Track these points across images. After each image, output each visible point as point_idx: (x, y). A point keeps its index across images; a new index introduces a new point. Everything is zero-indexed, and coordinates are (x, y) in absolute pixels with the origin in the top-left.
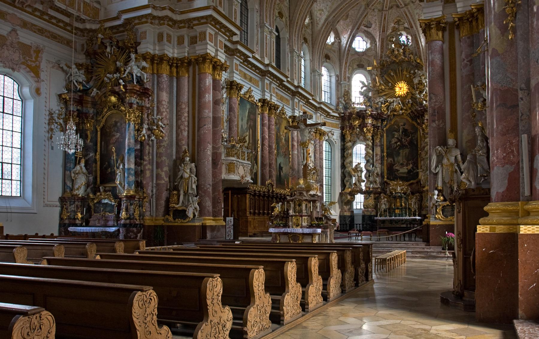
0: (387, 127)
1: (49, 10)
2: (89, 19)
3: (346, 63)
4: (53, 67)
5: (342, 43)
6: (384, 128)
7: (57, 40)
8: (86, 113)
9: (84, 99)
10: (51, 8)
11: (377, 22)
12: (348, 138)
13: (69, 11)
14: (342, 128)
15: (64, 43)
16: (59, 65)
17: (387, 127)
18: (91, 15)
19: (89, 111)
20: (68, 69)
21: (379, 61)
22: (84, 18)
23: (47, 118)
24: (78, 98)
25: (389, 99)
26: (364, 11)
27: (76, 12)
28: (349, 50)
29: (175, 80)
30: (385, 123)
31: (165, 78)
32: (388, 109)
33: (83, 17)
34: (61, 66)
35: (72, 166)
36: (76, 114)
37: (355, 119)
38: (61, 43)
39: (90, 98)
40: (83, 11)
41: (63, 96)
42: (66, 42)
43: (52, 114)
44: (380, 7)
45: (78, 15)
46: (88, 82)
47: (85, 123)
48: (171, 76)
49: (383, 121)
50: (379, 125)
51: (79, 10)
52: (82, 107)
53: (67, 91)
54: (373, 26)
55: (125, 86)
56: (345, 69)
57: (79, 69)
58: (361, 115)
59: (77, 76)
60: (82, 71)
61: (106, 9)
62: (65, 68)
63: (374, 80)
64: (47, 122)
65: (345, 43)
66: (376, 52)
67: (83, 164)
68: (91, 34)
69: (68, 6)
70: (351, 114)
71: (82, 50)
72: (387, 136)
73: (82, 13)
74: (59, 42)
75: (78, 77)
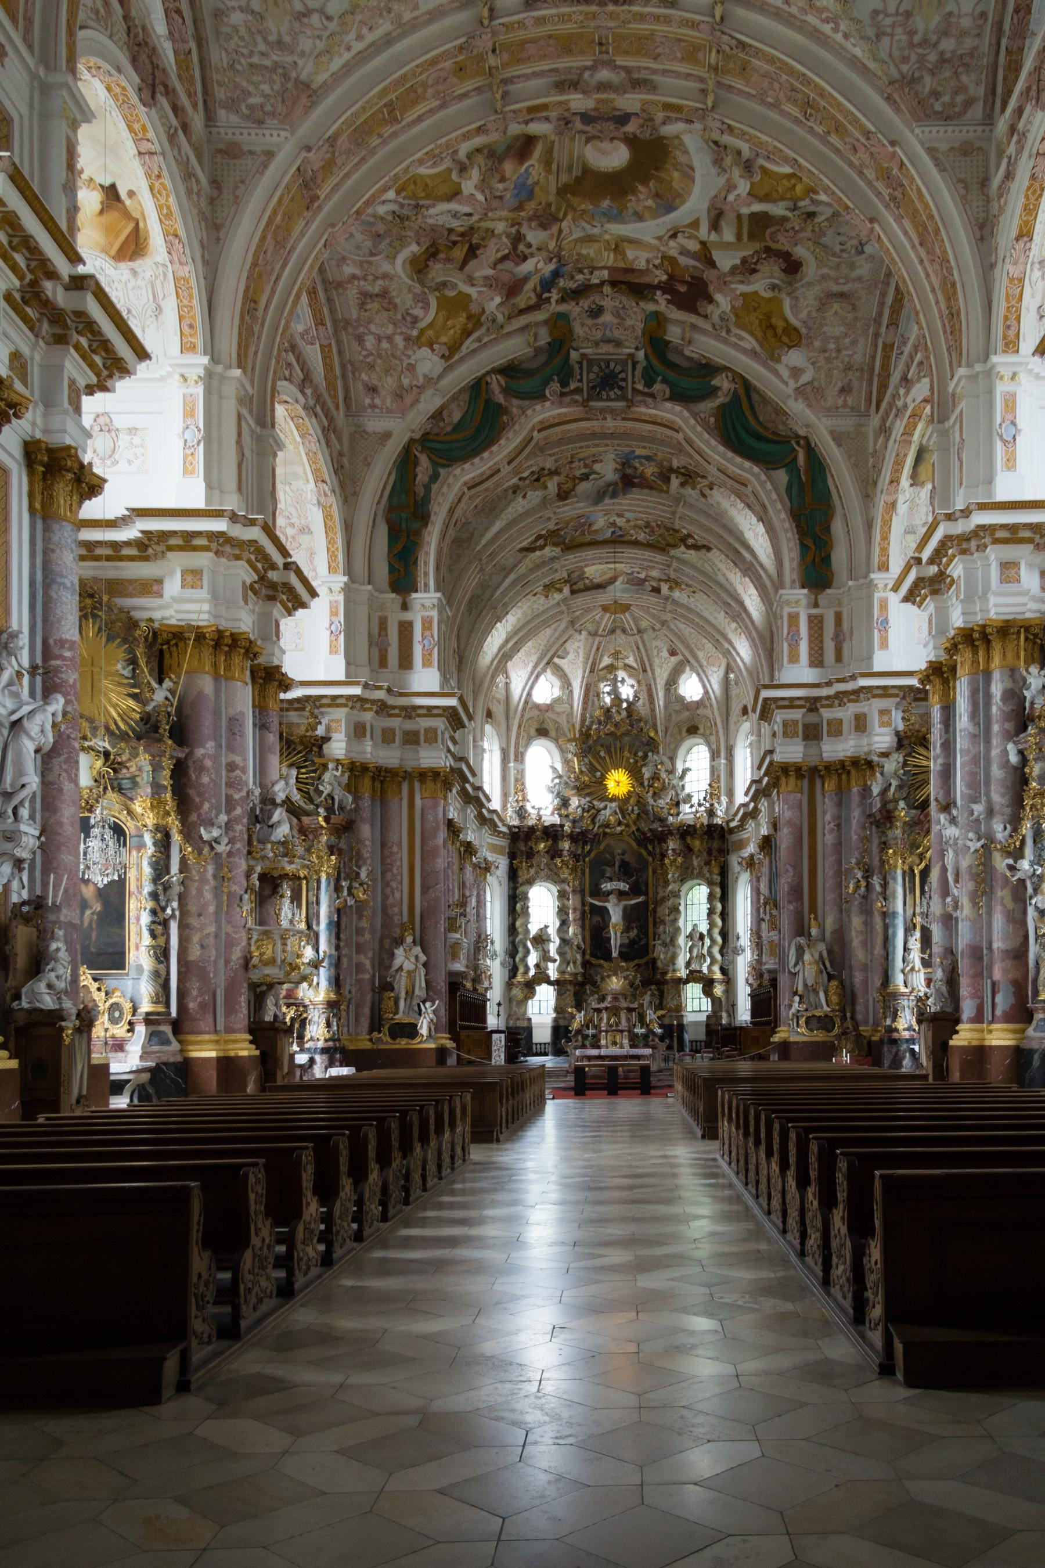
0: (593, 855)
3: (520, 726)
5: (513, 686)
6: (585, 856)
11: (581, 652)
12: (523, 876)
14: (512, 856)
17: (593, 855)
21: (577, 727)
25: (595, 803)
26: (564, 631)
28: (526, 702)
29: (378, 803)
30: (588, 848)
31: (366, 803)
32: (593, 822)
37: (537, 841)
44: (591, 628)
48: (373, 800)
49: (585, 843)
50: (579, 852)
54: (571, 657)
55: (327, 819)
56: (517, 738)
58: (551, 833)
63: (566, 762)
65: (521, 686)
66: (572, 707)
70: (532, 830)
72: (591, 873)
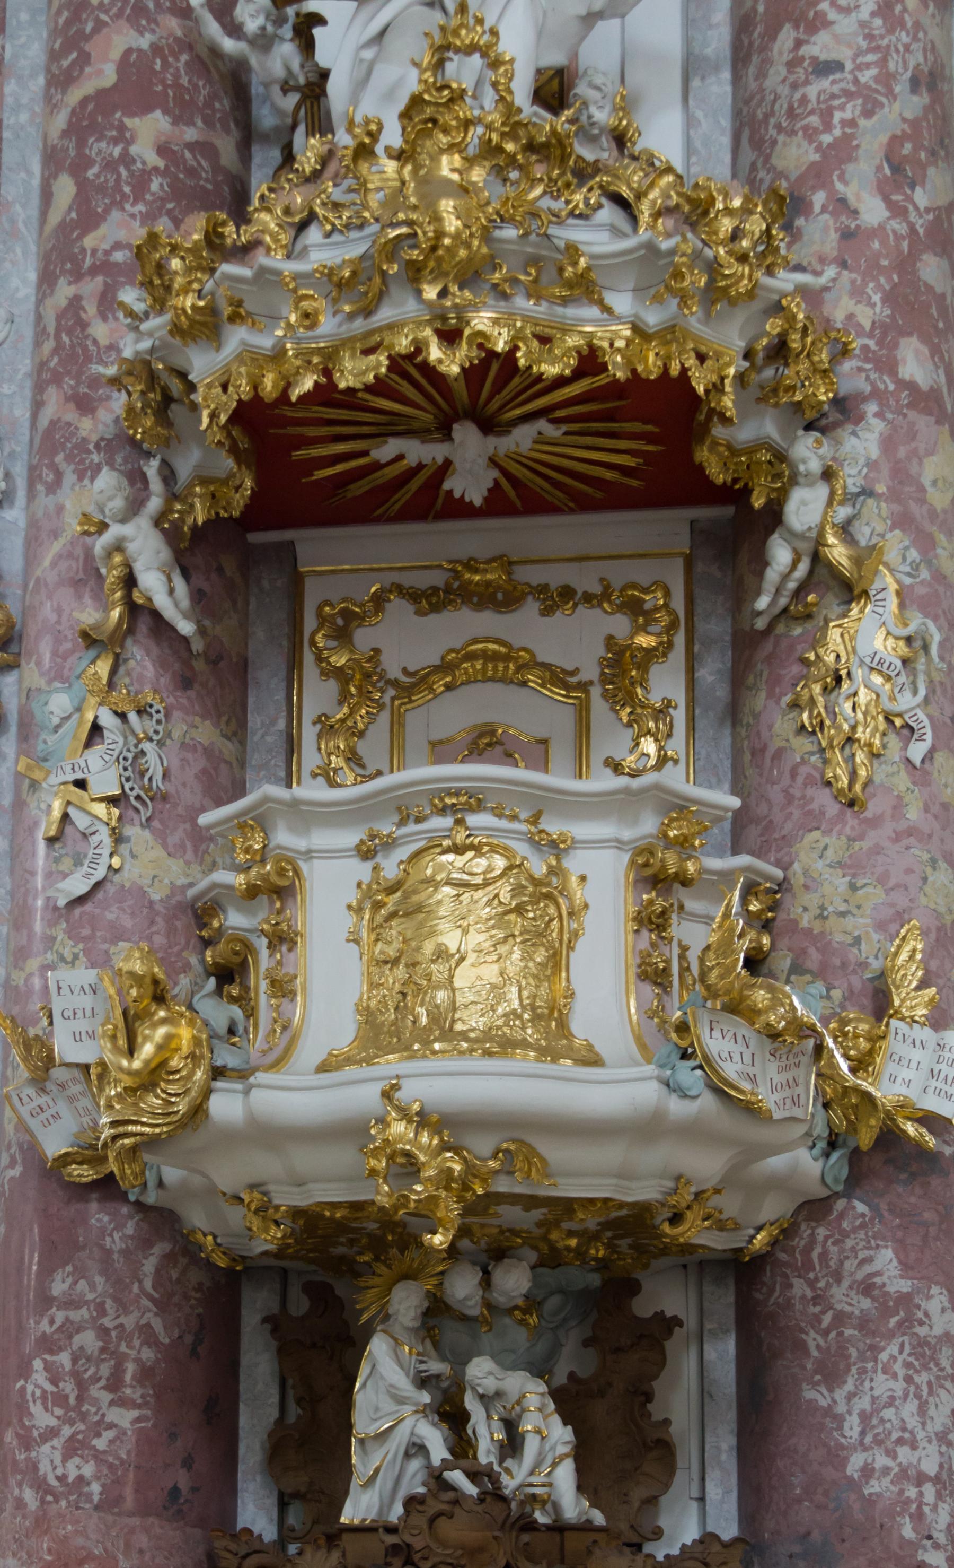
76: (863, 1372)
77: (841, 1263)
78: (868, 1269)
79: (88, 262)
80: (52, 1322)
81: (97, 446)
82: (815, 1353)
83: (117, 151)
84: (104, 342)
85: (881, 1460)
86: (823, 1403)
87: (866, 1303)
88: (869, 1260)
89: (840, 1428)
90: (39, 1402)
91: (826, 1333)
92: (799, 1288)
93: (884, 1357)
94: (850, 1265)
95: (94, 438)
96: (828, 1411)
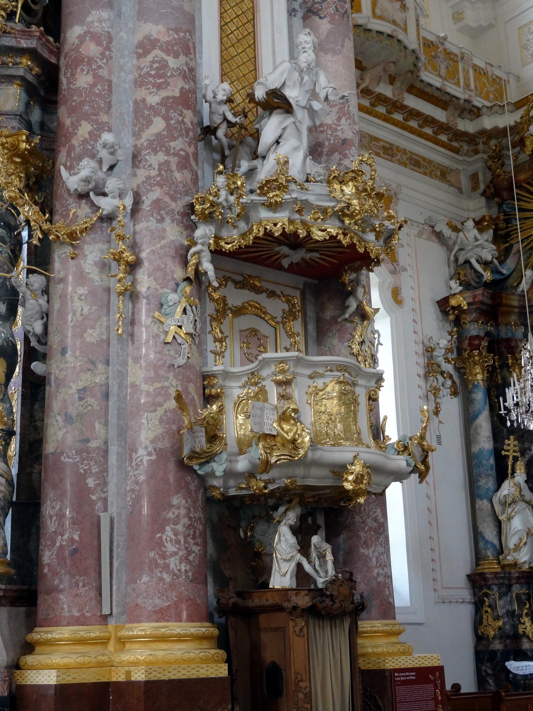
1: (406, 95)
2: (489, 104)
4: (420, 234)
7: (422, 170)
8: (508, 340)
9: (504, 301)
10: (412, 89)
13: (449, 90)
15: (436, 176)
16: (433, 227)
18: (491, 96)
19: (513, 334)
20: (454, 235)
22: (479, 105)
23: (422, 361)
24: (488, 301)
27: (461, 90)
33: (478, 102)
34: (437, 229)
35: (491, 484)
36: (485, 343)
38: (431, 177)
39: (515, 298)
40: (476, 87)
41: (453, 302)
42: (439, 173)
43: (433, 350)
45: (466, 97)
46: (501, 262)
47: (508, 367)
51: (467, 86)
52: (497, 325)
53: (461, 288)
57: (481, 231)
59: (477, 246)
60: (489, 234)
61: (518, 78)
62: (447, 232)
64: (422, 372)
67: (520, 476)
68: (493, 142)
69: (445, 79)
71: (475, 188)
73: (473, 94)
74: (425, 174)
75: (479, 249)
76: (376, 545)
77: (369, 512)
78: (375, 514)
79: (172, 151)
80: (174, 514)
81: (178, 213)
82: (363, 539)
83: (181, 118)
84: (179, 180)
85: (381, 571)
86: (366, 553)
87: (376, 524)
88: (375, 512)
89: (371, 561)
90: (169, 542)
91: (366, 532)
92: (358, 519)
93: (380, 540)
94: (371, 513)
95: (177, 210)
96: (368, 556)
